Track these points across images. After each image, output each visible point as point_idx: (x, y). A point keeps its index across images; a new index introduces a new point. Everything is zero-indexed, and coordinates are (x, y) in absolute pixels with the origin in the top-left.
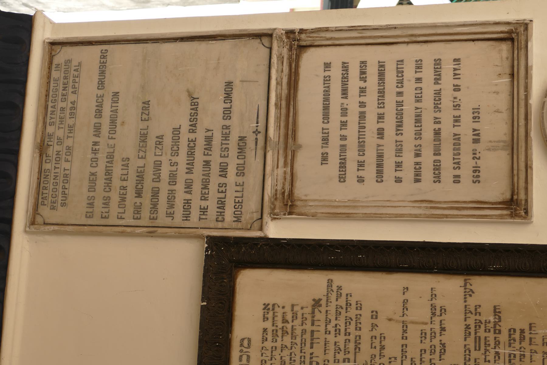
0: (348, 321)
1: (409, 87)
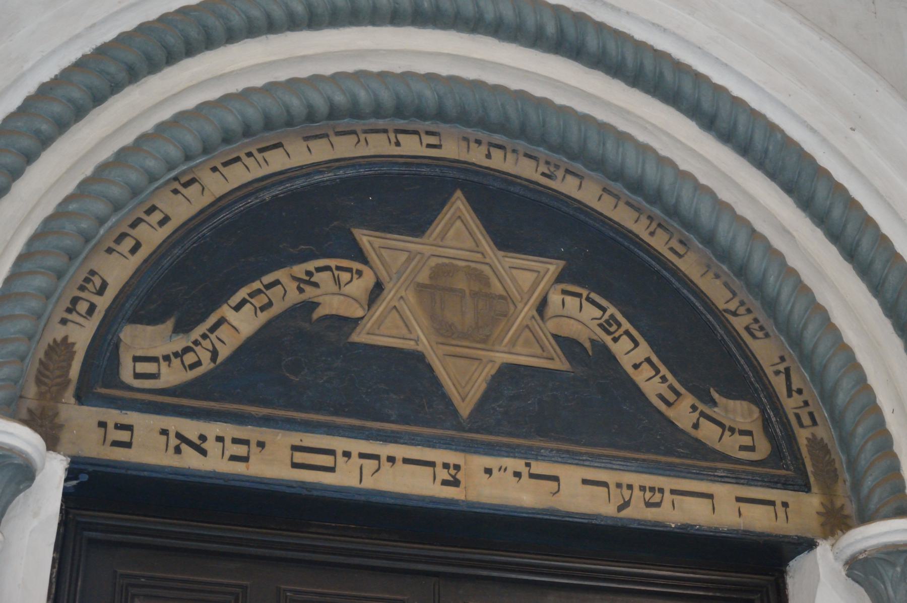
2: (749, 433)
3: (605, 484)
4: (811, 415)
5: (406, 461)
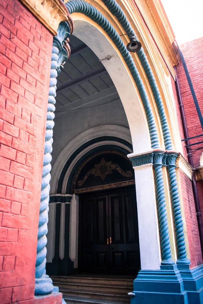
2: (130, 174)
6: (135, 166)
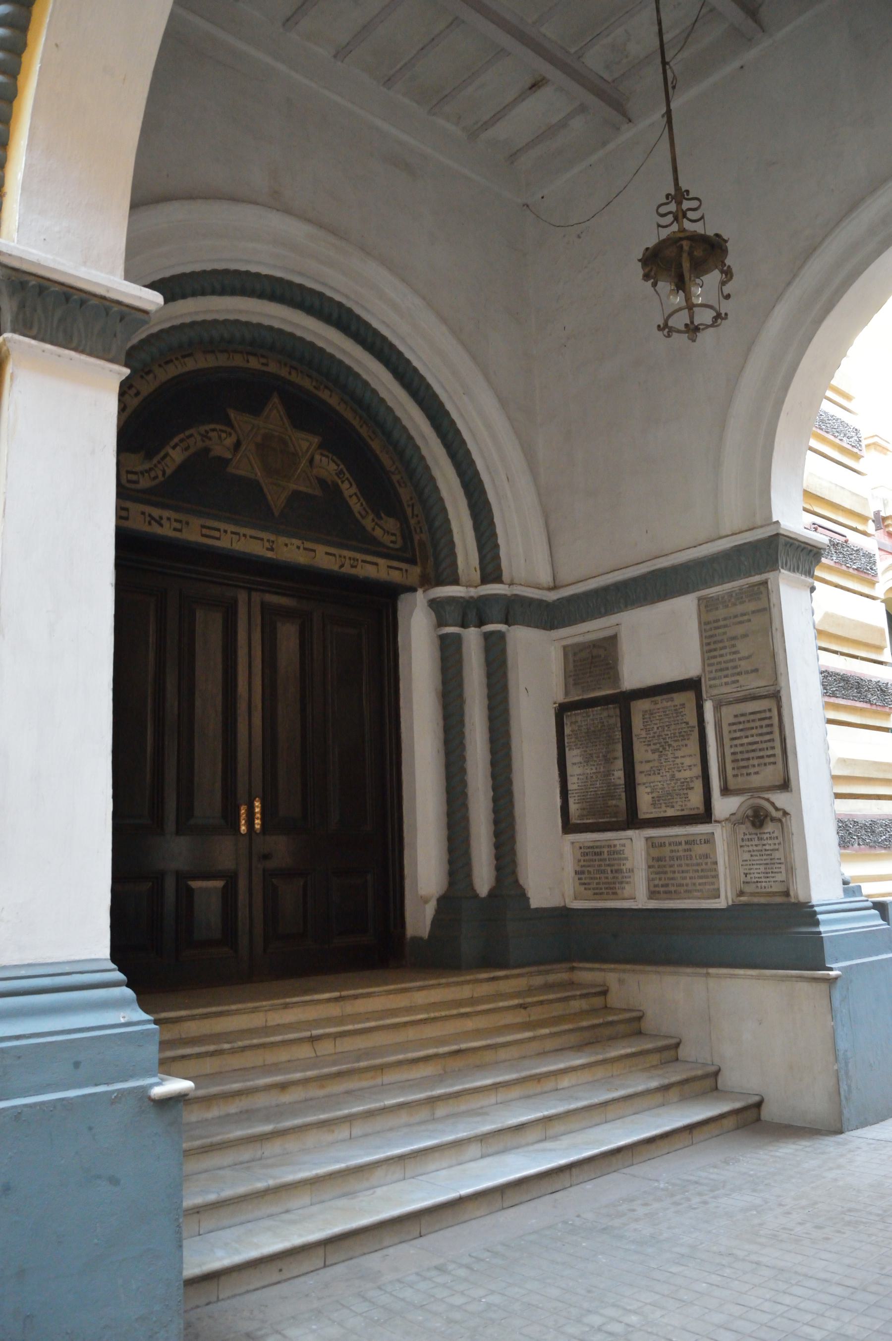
0: (683, 736)
1: (764, 745)
2: (393, 534)
3: (334, 555)
4: (421, 528)
5: (251, 537)
6: (782, 568)
